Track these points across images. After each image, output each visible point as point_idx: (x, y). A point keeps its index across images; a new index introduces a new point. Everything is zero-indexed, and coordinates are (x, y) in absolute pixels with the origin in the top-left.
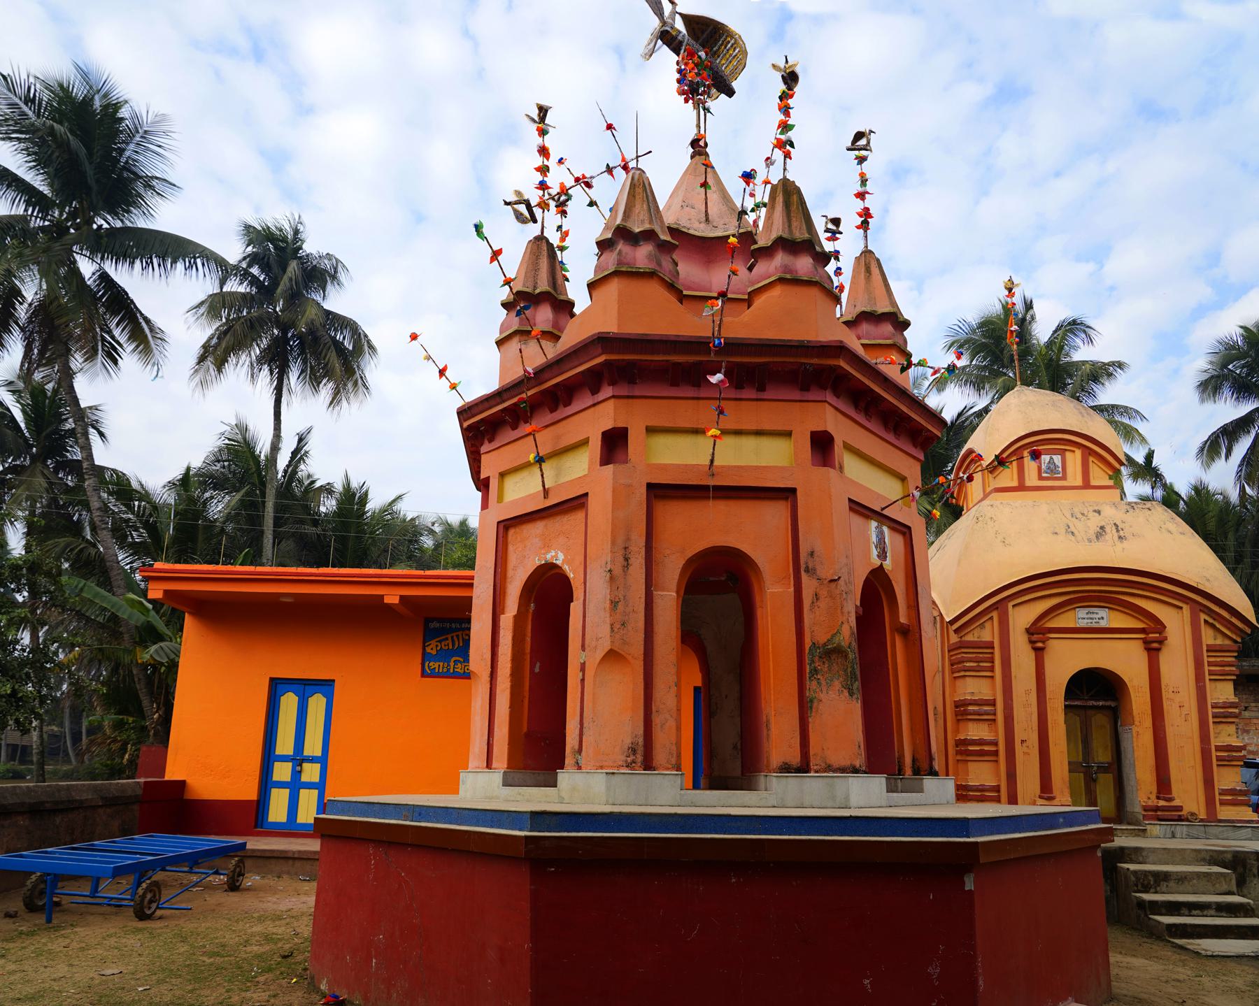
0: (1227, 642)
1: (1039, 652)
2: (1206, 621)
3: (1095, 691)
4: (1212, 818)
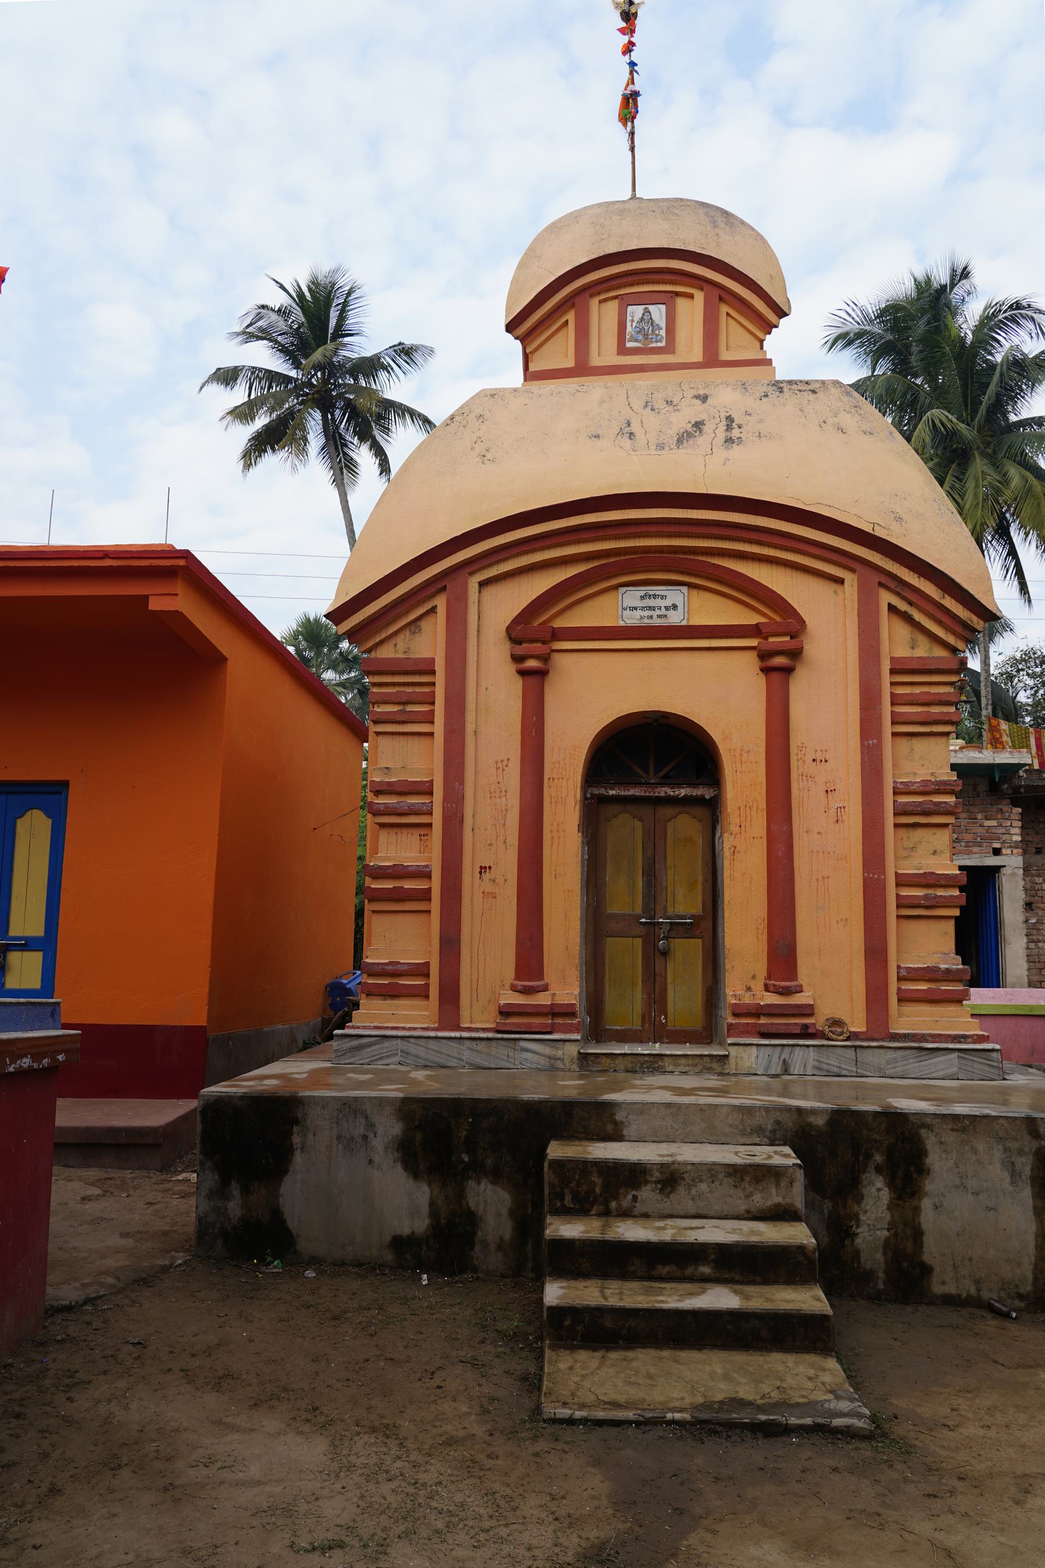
0: (940, 652)
1: (535, 678)
2: (891, 608)
3: (655, 762)
4: (879, 1030)
